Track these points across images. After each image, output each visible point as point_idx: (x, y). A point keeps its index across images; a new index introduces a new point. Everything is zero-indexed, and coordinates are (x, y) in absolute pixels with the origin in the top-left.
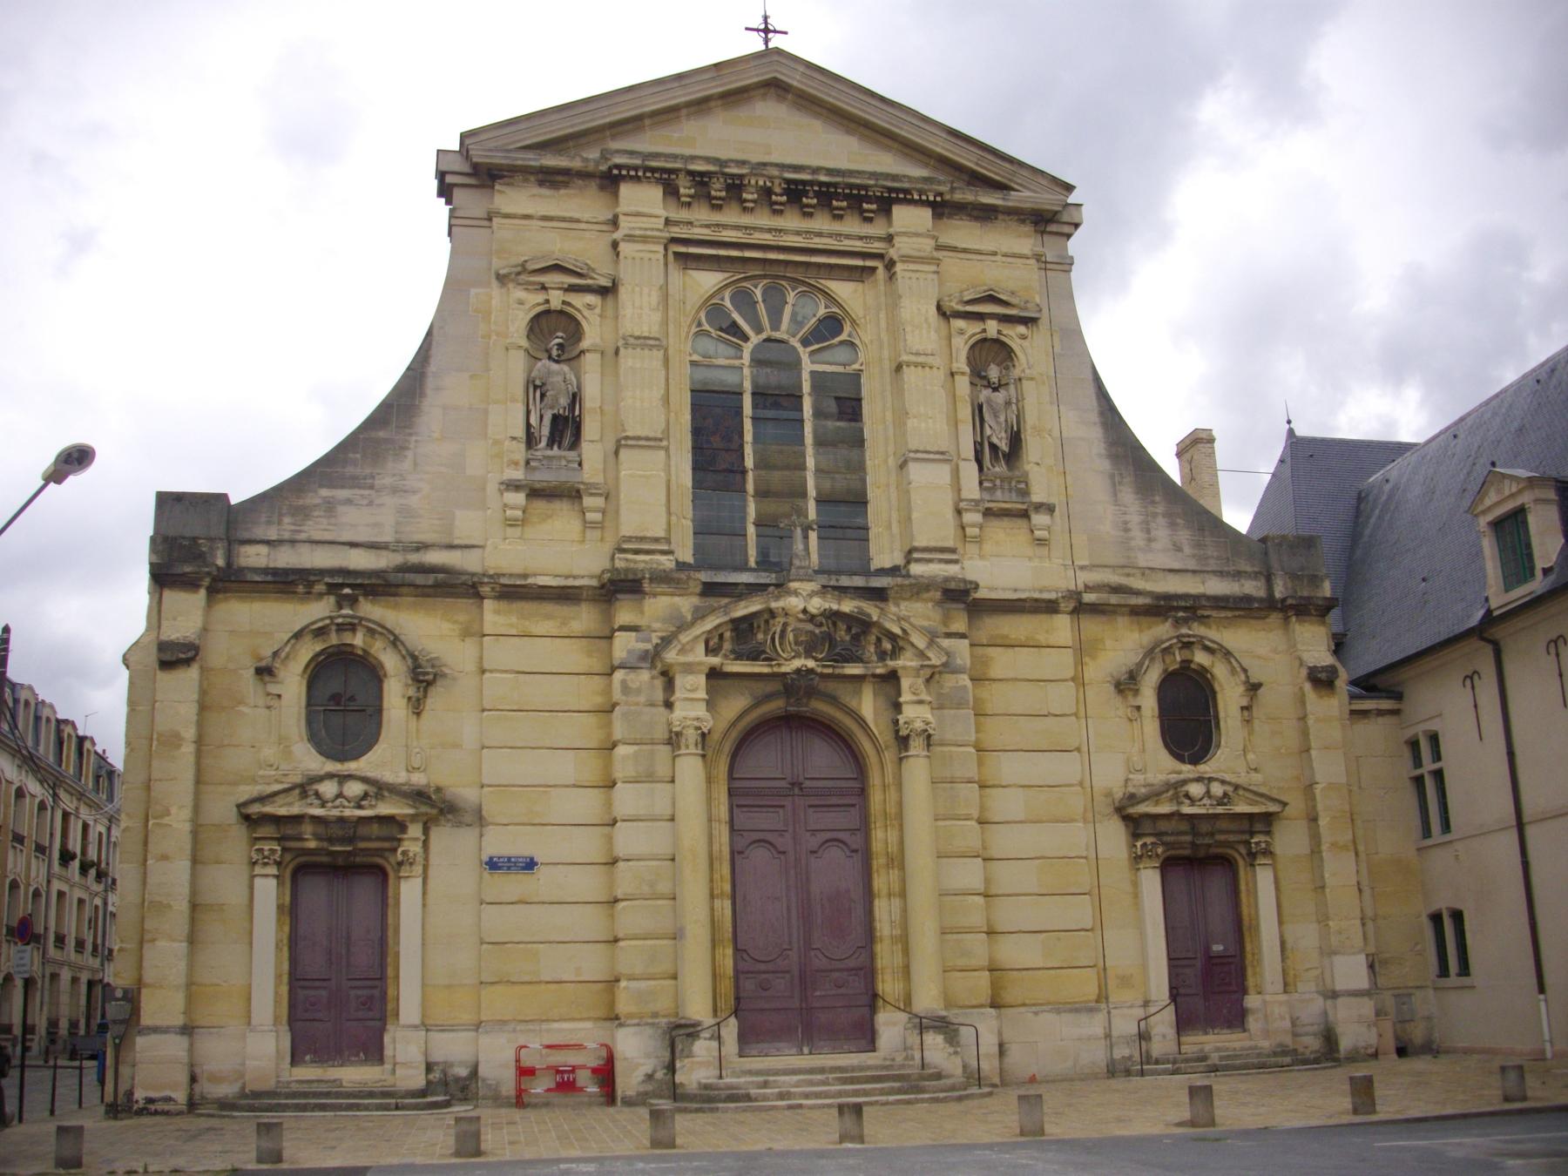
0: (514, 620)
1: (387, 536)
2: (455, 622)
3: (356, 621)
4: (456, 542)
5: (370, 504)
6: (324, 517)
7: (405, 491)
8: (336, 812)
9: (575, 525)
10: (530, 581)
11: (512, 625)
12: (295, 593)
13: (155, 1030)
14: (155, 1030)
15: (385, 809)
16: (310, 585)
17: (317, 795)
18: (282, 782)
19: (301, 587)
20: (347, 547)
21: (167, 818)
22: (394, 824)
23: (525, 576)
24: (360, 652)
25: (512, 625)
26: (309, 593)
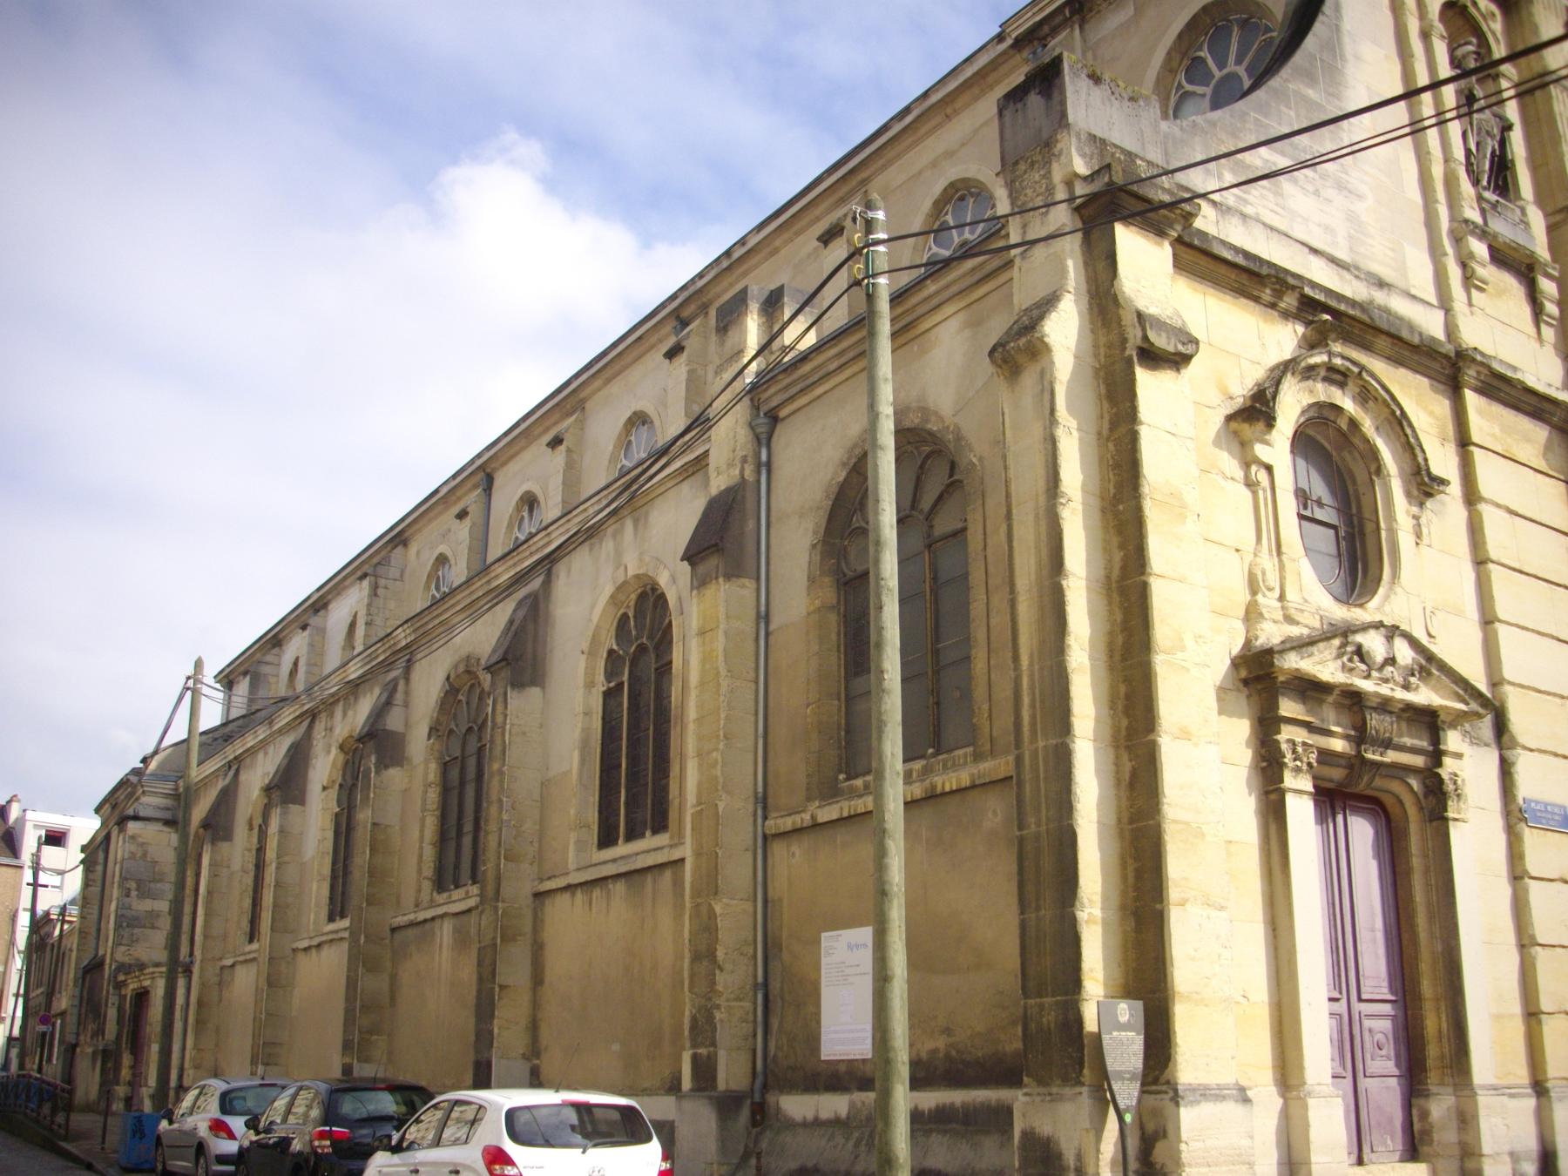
0: (1497, 430)
1: (1342, 255)
2: (1431, 414)
3: (1356, 370)
4: (1413, 292)
5: (1317, 193)
6: (1269, 190)
7: (1350, 192)
8: (1385, 690)
9: (1526, 311)
10: (1518, 376)
11: (1493, 435)
12: (1256, 299)
13: (1207, 1093)
14: (1207, 1093)
15: (1424, 696)
16: (1279, 294)
17: (1360, 652)
18: (1298, 623)
19: (1268, 291)
20: (1307, 250)
21: (1180, 655)
22: (1429, 721)
23: (1515, 369)
24: (1344, 425)
25: (1493, 435)
26: (1273, 306)
